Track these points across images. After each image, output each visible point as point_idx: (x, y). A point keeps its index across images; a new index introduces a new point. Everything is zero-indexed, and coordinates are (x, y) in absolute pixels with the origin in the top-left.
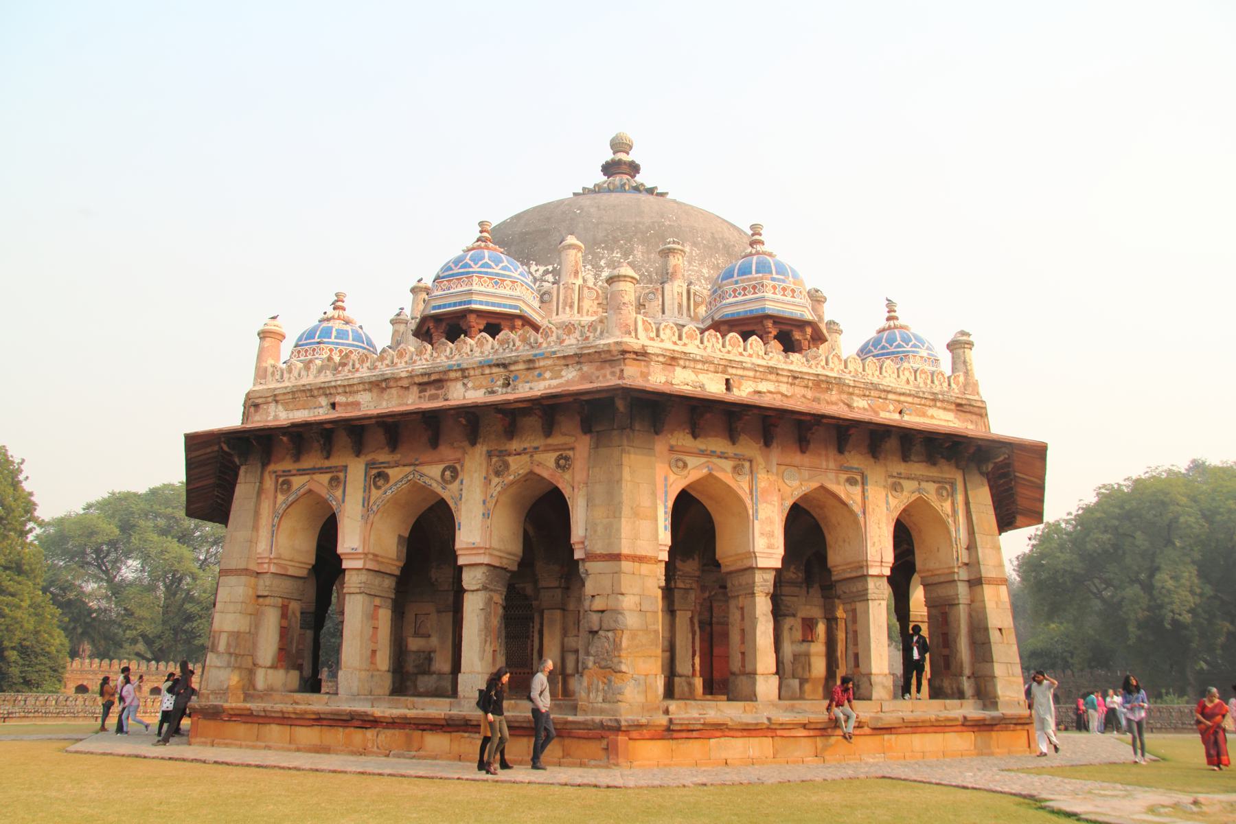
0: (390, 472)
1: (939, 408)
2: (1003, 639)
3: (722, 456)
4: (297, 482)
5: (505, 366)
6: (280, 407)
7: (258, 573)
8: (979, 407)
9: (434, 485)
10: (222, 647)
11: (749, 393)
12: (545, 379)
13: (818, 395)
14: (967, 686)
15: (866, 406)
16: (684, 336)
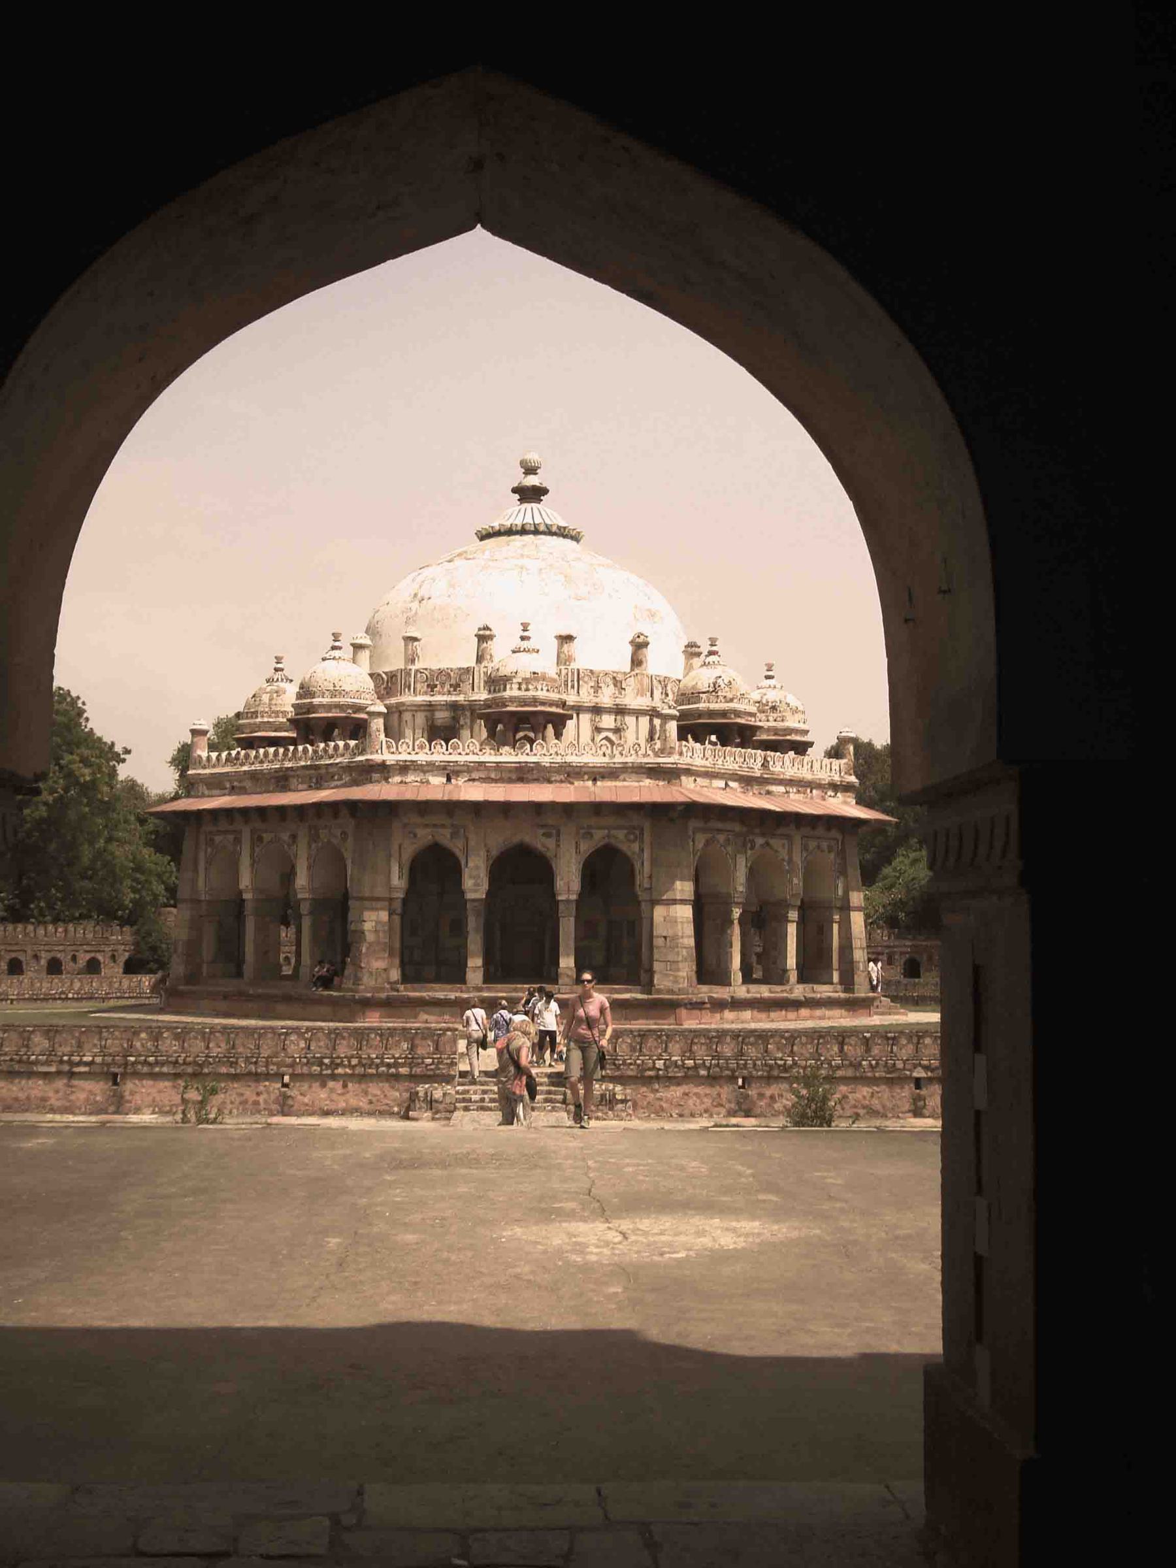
0: (264, 835)
1: (632, 772)
2: (665, 944)
3: (443, 826)
4: (218, 839)
5: (315, 770)
6: (205, 787)
7: (200, 901)
8: (670, 768)
9: (286, 846)
10: (180, 950)
11: (465, 781)
12: (335, 780)
13: (521, 775)
14: (644, 977)
15: (563, 779)
16: (416, 747)
